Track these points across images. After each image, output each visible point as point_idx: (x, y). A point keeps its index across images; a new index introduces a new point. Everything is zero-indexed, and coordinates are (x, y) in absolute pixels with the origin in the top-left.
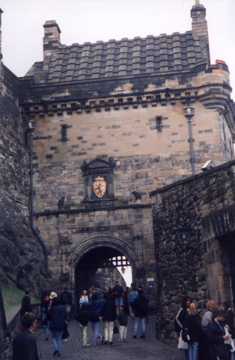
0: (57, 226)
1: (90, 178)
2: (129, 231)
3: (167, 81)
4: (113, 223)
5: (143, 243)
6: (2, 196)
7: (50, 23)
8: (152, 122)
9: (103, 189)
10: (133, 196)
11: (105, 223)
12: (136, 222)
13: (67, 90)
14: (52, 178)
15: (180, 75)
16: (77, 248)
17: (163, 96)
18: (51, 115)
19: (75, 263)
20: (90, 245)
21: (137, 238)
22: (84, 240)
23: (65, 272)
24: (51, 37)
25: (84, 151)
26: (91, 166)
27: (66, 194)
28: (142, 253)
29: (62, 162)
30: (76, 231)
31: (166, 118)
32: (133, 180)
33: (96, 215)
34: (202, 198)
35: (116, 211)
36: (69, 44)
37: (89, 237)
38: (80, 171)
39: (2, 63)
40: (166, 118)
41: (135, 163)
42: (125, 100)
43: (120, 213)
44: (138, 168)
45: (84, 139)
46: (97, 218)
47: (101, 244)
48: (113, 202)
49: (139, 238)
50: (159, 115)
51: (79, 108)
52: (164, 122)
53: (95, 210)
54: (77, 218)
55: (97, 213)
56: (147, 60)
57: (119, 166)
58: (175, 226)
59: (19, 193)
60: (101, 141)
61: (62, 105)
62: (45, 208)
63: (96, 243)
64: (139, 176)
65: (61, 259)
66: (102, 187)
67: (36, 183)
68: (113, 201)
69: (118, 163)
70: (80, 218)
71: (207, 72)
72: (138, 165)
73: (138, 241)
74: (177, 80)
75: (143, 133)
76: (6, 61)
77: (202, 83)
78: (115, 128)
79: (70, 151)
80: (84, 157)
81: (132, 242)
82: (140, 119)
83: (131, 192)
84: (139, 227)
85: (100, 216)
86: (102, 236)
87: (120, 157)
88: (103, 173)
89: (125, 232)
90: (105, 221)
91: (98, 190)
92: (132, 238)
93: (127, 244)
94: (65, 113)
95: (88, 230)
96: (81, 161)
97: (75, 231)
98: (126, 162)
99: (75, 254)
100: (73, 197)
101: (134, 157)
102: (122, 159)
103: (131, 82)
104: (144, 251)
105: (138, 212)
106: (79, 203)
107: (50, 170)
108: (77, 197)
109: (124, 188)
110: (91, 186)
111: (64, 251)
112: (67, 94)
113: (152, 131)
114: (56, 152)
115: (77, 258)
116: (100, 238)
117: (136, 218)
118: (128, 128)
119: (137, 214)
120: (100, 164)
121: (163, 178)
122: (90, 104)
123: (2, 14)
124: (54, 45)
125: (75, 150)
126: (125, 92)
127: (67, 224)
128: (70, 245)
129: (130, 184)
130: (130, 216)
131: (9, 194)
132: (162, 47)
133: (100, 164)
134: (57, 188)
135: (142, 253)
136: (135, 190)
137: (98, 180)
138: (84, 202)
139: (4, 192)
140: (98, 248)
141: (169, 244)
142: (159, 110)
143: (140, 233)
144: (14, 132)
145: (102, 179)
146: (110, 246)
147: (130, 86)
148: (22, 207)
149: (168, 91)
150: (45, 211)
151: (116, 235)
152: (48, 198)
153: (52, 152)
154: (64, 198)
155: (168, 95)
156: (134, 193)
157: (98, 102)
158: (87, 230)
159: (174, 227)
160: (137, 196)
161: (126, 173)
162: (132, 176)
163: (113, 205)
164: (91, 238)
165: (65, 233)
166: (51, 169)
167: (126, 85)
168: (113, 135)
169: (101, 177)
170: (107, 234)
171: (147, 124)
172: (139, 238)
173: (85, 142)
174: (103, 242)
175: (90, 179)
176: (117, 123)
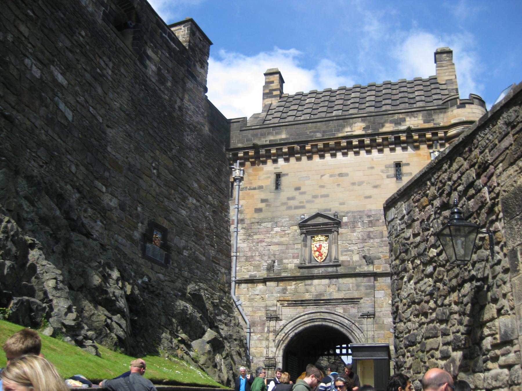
0: (263, 296)
1: (309, 237)
3: (408, 119)
4: (336, 295)
6: (191, 249)
7: (272, 71)
8: (390, 169)
9: (325, 250)
10: (364, 260)
12: (367, 295)
13: (284, 132)
14: (261, 237)
15: (425, 112)
16: (287, 327)
17: (403, 137)
18: (264, 163)
19: (284, 345)
20: (304, 322)
21: (367, 315)
22: (297, 316)
23: (271, 356)
24: (272, 85)
25: (302, 205)
26: (309, 223)
27: (276, 256)
28: (374, 335)
29: (274, 218)
31: (408, 164)
32: (364, 241)
33: (314, 284)
34: (501, 159)
35: (340, 280)
36: (292, 93)
37: (304, 312)
38: (296, 228)
39: (206, 97)
40: (408, 164)
41: (366, 220)
42: (355, 142)
44: (371, 226)
45: (302, 190)
46: (315, 287)
50: (397, 160)
51: (298, 153)
52: (404, 169)
53: (312, 278)
54: (289, 287)
55: (316, 282)
56: (383, 103)
57: (346, 224)
58: (434, 246)
59: (217, 251)
60: (324, 191)
61: (277, 149)
62: (250, 273)
64: (372, 236)
65: (267, 339)
67: (241, 241)
68: (336, 266)
69: (345, 219)
70: (293, 287)
71: (459, 107)
72: (370, 222)
73: (369, 319)
74: (421, 118)
75: (377, 183)
76: (210, 96)
77: (453, 121)
78: (342, 176)
79: (284, 204)
80: (302, 211)
81: (360, 321)
82: (374, 166)
84: (370, 301)
85: (318, 287)
87: (348, 213)
89: (352, 307)
91: (317, 253)
92: (361, 316)
93: (353, 323)
94: (281, 161)
95: (302, 303)
98: (354, 217)
100: (285, 261)
101: (366, 213)
102: (349, 214)
103: (363, 121)
104: (376, 332)
106: (293, 268)
107: (259, 227)
108: (290, 260)
109: (352, 251)
111: (271, 329)
112: (283, 136)
113: (389, 179)
114: (267, 205)
116: (318, 314)
117: (367, 289)
118: (358, 176)
120: (321, 220)
122: (312, 148)
123: (211, 46)
124: (275, 93)
125: (292, 203)
126: (355, 133)
127: (275, 295)
128: (279, 322)
129: (360, 245)
130: (358, 286)
131: (202, 250)
132: (402, 90)
133: (321, 220)
134: (266, 249)
135: (374, 335)
139: (194, 246)
141: (418, 285)
142: (399, 154)
143: (371, 310)
144: (216, 179)
145: (323, 238)
146: (331, 325)
147: (361, 126)
148: (220, 269)
149: (409, 131)
150: (250, 276)
152: (255, 260)
153: (262, 205)
154: (274, 262)
155: (409, 136)
156: (364, 257)
157: (321, 145)
159: (429, 249)
160: (369, 260)
161: (354, 231)
162: (362, 236)
163: (337, 271)
164: (307, 314)
165: (273, 305)
166: (260, 225)
167: (356, 125)
168: (339, 185)
171: (382, 171)
172: (370, 315)
173: (304, 193)
176: (344, 171)
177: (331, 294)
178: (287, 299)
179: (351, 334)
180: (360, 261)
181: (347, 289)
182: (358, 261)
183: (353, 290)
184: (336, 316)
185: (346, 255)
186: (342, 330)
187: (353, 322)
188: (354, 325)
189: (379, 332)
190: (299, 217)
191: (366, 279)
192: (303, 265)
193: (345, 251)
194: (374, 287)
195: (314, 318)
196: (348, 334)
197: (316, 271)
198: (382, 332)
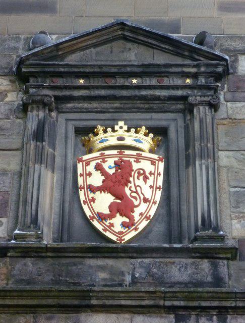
9: (147, 190)
26: (73, 59)
66: (140, 182)
88: (150, 104)
96: (17, 39)
110: (65, 170)
133: (134, 55)
137: (113, 140)
163: (218, 281)
169: (133, 127)
175: (61, 131)
190: (21, 45)
192: (32, 242)
197: (98, 272)
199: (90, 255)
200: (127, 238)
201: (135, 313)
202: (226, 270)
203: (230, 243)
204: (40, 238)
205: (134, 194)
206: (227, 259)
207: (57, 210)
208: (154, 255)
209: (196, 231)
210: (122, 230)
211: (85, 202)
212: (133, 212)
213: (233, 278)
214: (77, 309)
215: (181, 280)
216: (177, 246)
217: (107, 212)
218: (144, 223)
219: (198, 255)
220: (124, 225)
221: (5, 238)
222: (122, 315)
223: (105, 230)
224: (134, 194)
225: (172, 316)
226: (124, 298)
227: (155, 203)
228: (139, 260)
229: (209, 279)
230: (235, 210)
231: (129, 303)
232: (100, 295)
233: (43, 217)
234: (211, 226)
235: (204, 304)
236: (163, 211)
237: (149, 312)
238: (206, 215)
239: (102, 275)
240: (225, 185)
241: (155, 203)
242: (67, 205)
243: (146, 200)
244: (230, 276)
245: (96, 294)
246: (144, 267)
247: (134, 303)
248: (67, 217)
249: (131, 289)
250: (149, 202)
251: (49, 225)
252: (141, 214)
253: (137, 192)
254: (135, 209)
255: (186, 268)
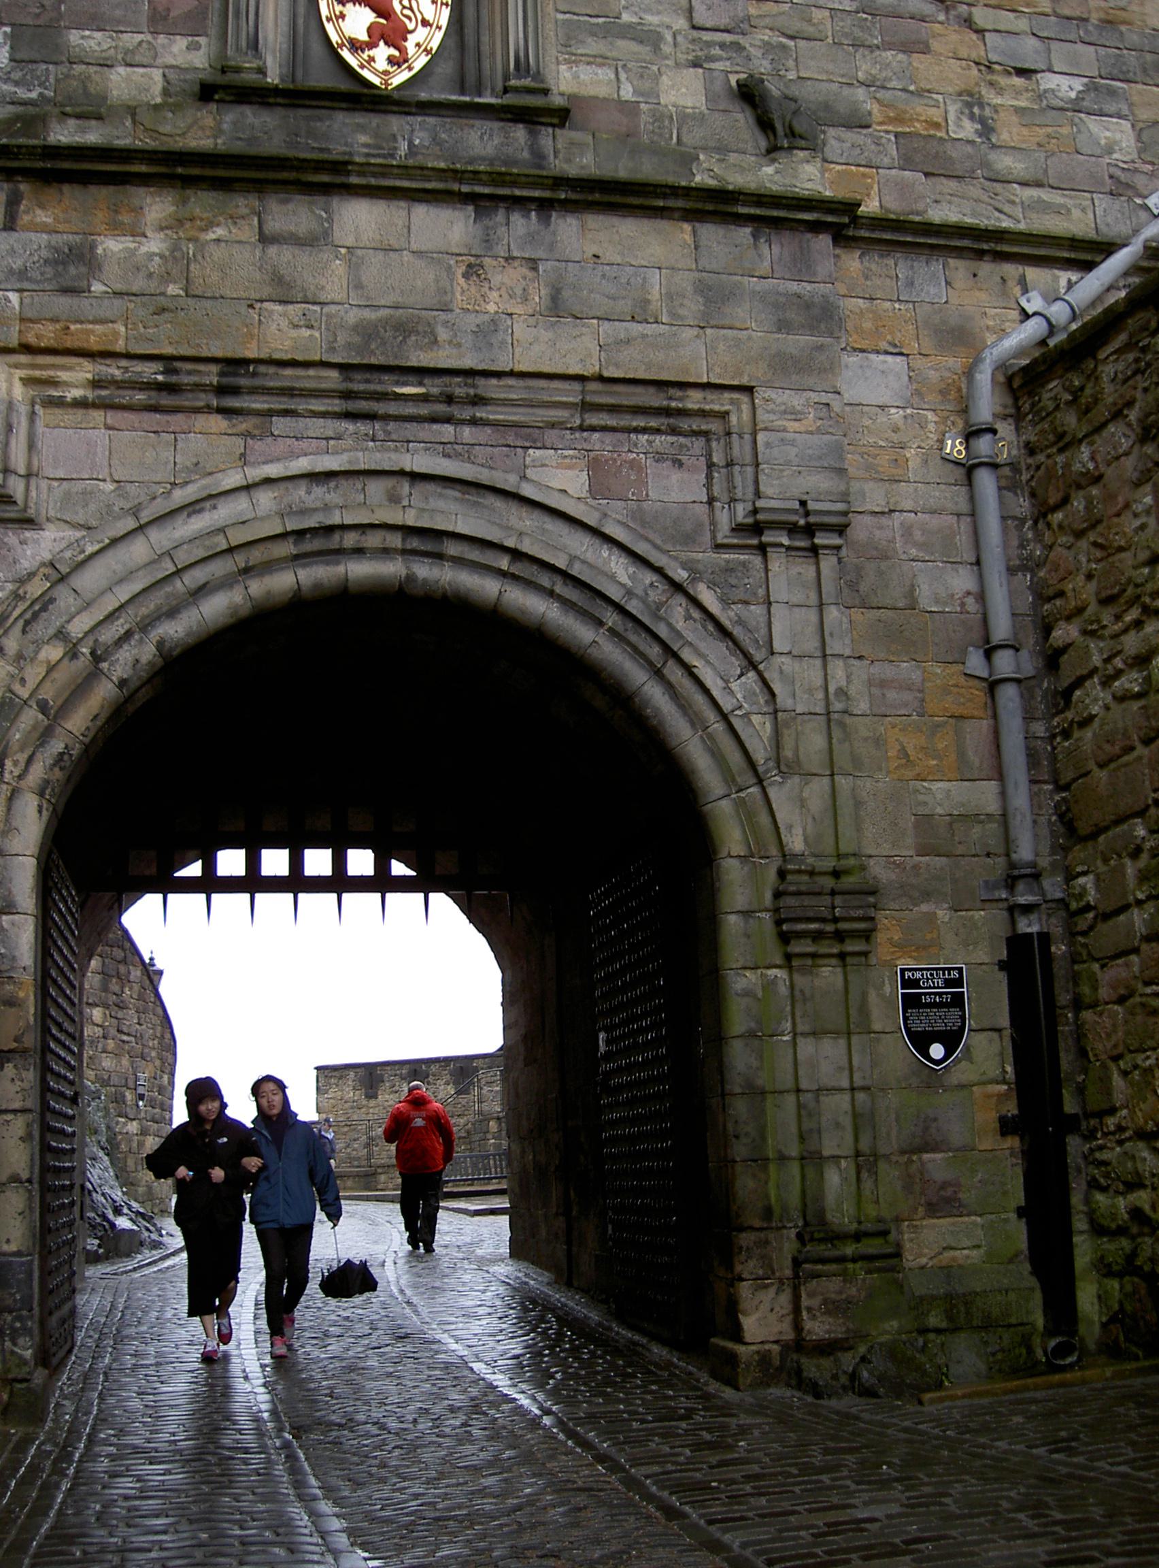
2: (698, 444)
4: (534, 346)
5: (855, 594)
10: (742, 118)
11: (443, 334)
12: (787, 367)
16: (88, 580)
19: (56, 746)
20: (245, 556)
21: (792, 529)
22: (180, 496)
30: (96, 384)
43: (610, 255)
47: (386, 552)
48: (533, 134)
49: (810, 531)
54: (112, 246)
55: (359, 219)
63: (318, 540)
70: (155, 244)
81: (729, 569)
83: (718, 86)
84: (810, 421)
86: (402, 473)
89: (659, 457)
90: (446, 309)
92: (738, 529)
93: (677, 587)
97: (76, 378)
99: (61, 635)
105: (802, 268)
109: (651, 39)
115: (80, 689)
116: (376, 488)
117: (783, 326)
119: (794, 287)
121: (1022, 24)
136: (762, 66)
138: (219, 90)
140: (344, 600)
143: (816, 486)
146: (487, 588)
151: (560, 476)
158: (221, 390)
164: (268, 481)
170: (447, 450)
172: (810, 530)
174: (409, 531)
177: (487, 332)
178: (95, 336)
179: (658, 674)
180: (718, 120)
181: (624, 306)
182: (700, 118)
183: (677, 321)
184: (528, 521)
185: (599, 60)
186: (581, 633)
187: (681, 575)
188: (678, 610)
189: (888, 671)
191: (772, 252)
193: (594, 31)
194: (822, 317)
195: (336, 519)
196: (636, 676)
198: (906, 670)
199: (344, 105)
200: (397, 81)
201: (414, 200)
202: (551, 143)
203: (557, 101)
204: (262, 71)
205: (407, 12)
206: (553, 126)
207: (286, 29)
208: (444, 112)
209: (506, 77)
210: (389, 68)
211: (329, 19)
212: (405, 40)
213: (561, 156)
214: (326, 189)
215: (483, 153)
216: (477, 100)
217: (364, 37)
218: (423, 60)
219: (509, 116)
220: (391, 60)
221: (204, 69)
222: (396, 203)
223: (362, 67)
224: (407, 12)
225: (471, 208)
226: (400, 177)
227: (439, 28)
228: (419, 119)
229: (526, 154)
230: (564, 50)
231: (406, 184)
232: (364, 169)
233: (265, 39)
234: (528, 71)
235: (517, 192)
236: (451, 43)
237: (437, 200)
238: (522, 54)
239: (363, 139)
240: (550, 8)
241: (439, 28)
242: (301, 21)
243: (425, 23)
244: (556, 153)
245: (356, 168)
246: (427, 130)
247: (414, 185)
248: (300, 42)
249: (411, 162)
250: (431, 26)
251: (274, 52)
252: (418, 45)
253: (411, 9)
254: (409, 36)
255: (491, 136)
